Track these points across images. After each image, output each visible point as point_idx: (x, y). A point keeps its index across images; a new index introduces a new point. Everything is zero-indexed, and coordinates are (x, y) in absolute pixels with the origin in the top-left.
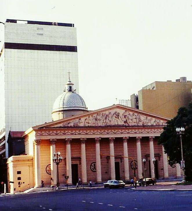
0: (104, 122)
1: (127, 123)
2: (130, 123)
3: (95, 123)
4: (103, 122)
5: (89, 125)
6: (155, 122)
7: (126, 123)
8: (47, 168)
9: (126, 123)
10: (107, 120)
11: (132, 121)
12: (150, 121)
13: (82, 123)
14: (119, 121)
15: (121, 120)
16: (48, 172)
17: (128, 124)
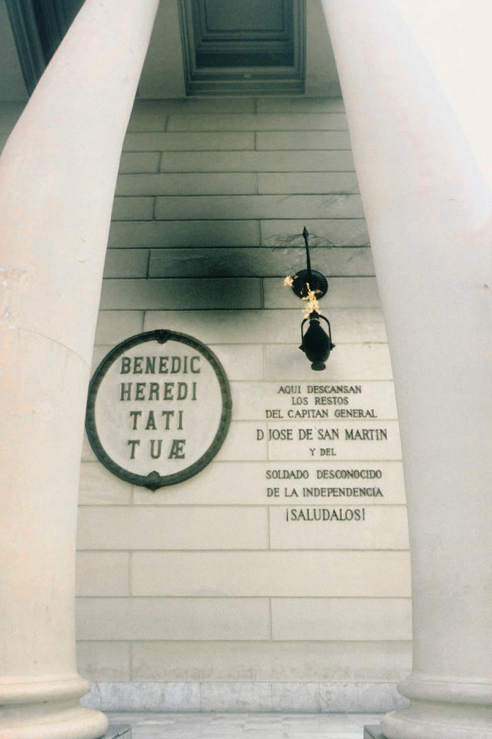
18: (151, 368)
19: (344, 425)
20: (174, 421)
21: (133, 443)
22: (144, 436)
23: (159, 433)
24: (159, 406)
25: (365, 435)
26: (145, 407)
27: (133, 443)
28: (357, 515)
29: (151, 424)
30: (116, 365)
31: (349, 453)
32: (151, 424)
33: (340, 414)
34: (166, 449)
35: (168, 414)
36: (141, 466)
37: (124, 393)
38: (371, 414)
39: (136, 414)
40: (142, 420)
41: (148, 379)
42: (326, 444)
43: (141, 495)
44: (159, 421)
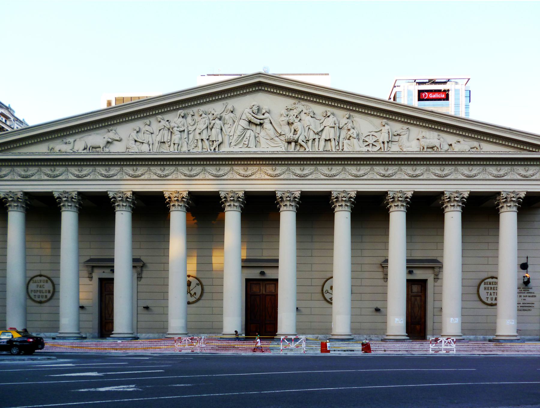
0: (202, 140)
1: (296, 142)
2: (310, 143)
3: (165, 140)
4: (198, 137)
5: (145, 148)
6: (418, 139)
7: (293, 144)
8: (31, 283)
9: (293, 144)
10: (213, 129)
11: (317, 137)
12: (397, 137)
13: (117, 140)
14: (263, 134)
15: (272, 132)
16: (32, 295)
17: (301, 146)
18: (490, 284)
19: (528, 295)
20: (495, 294)
21: (488, 298)
22: (489, 297)
23: (492, 296)
24: (492, 291)
25: (532, 296)
26: (490, 291)
27: (488, 298)
28: (530, 310)
29: (491, 294)
30: (483, 283)
31: (529, 300)
32: (491, 294)
33: (528, 293)
34: (494, 299)
35: (494, 293)
36: (489, 302)
37: (485, 289)
38: (533, 293)
39: (488, 293)
40: (489, 294)
41: (490, 286)
42: (525, 298)
43: (489, 307)
44: (492, 294)
